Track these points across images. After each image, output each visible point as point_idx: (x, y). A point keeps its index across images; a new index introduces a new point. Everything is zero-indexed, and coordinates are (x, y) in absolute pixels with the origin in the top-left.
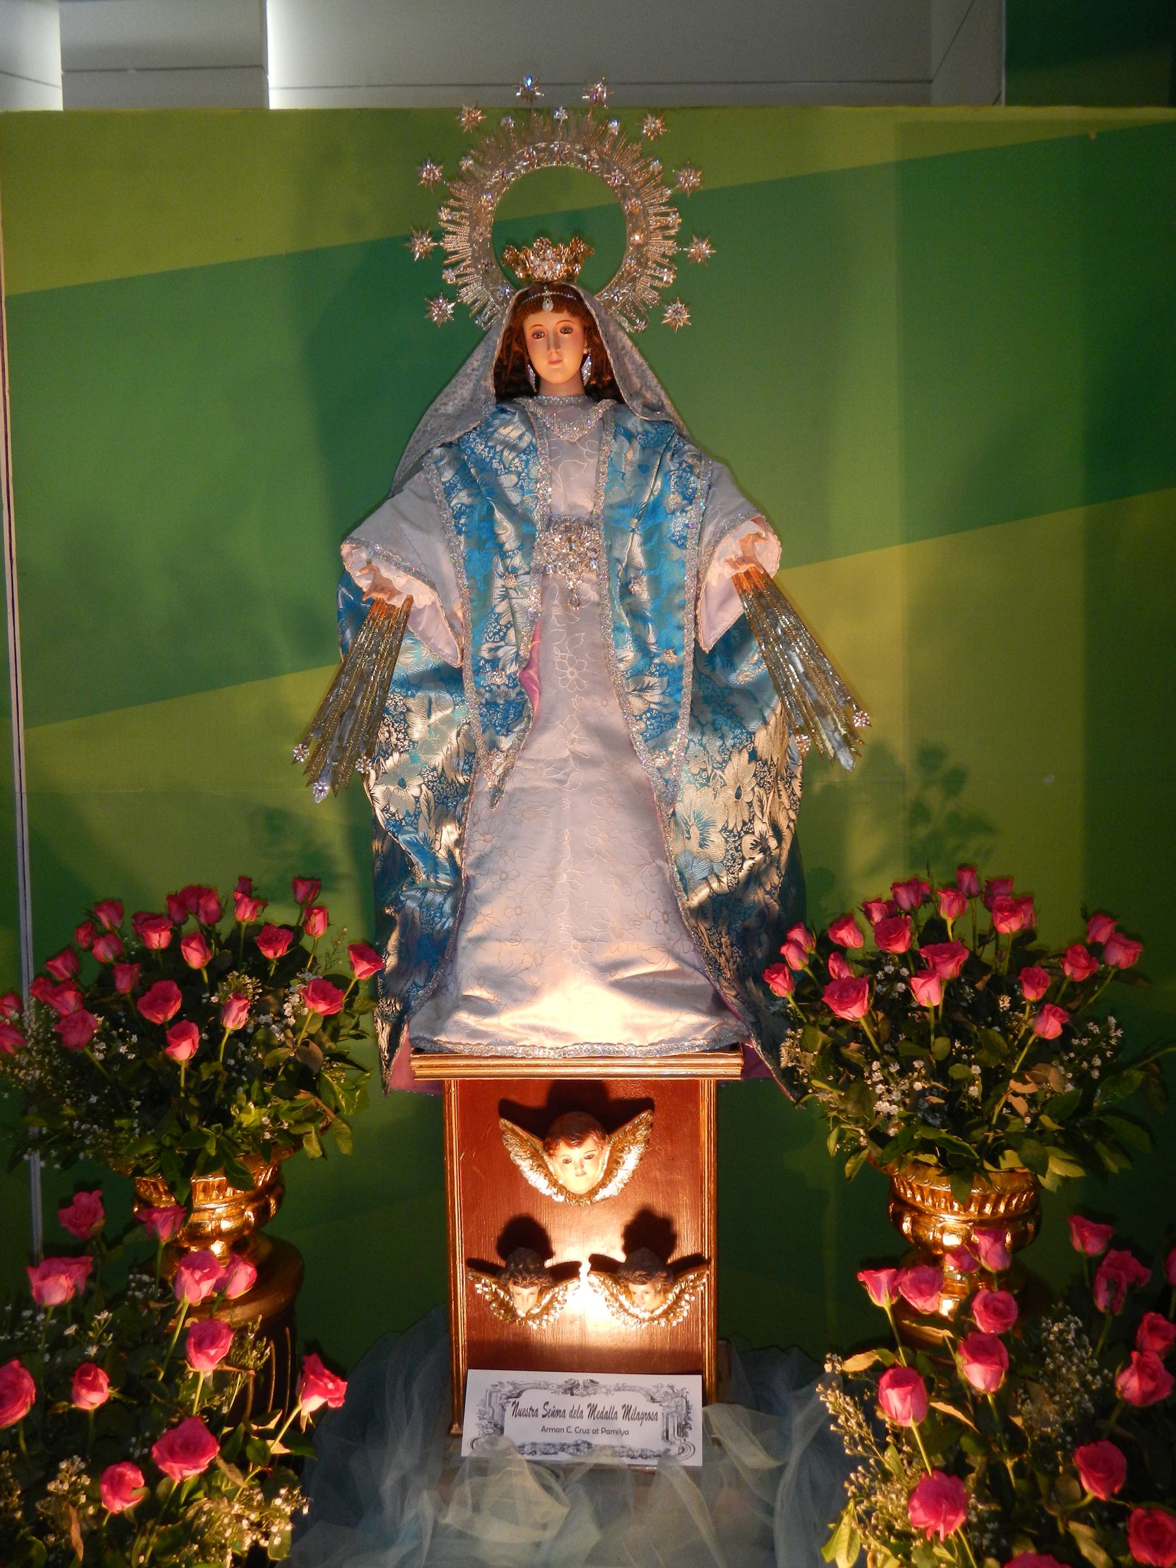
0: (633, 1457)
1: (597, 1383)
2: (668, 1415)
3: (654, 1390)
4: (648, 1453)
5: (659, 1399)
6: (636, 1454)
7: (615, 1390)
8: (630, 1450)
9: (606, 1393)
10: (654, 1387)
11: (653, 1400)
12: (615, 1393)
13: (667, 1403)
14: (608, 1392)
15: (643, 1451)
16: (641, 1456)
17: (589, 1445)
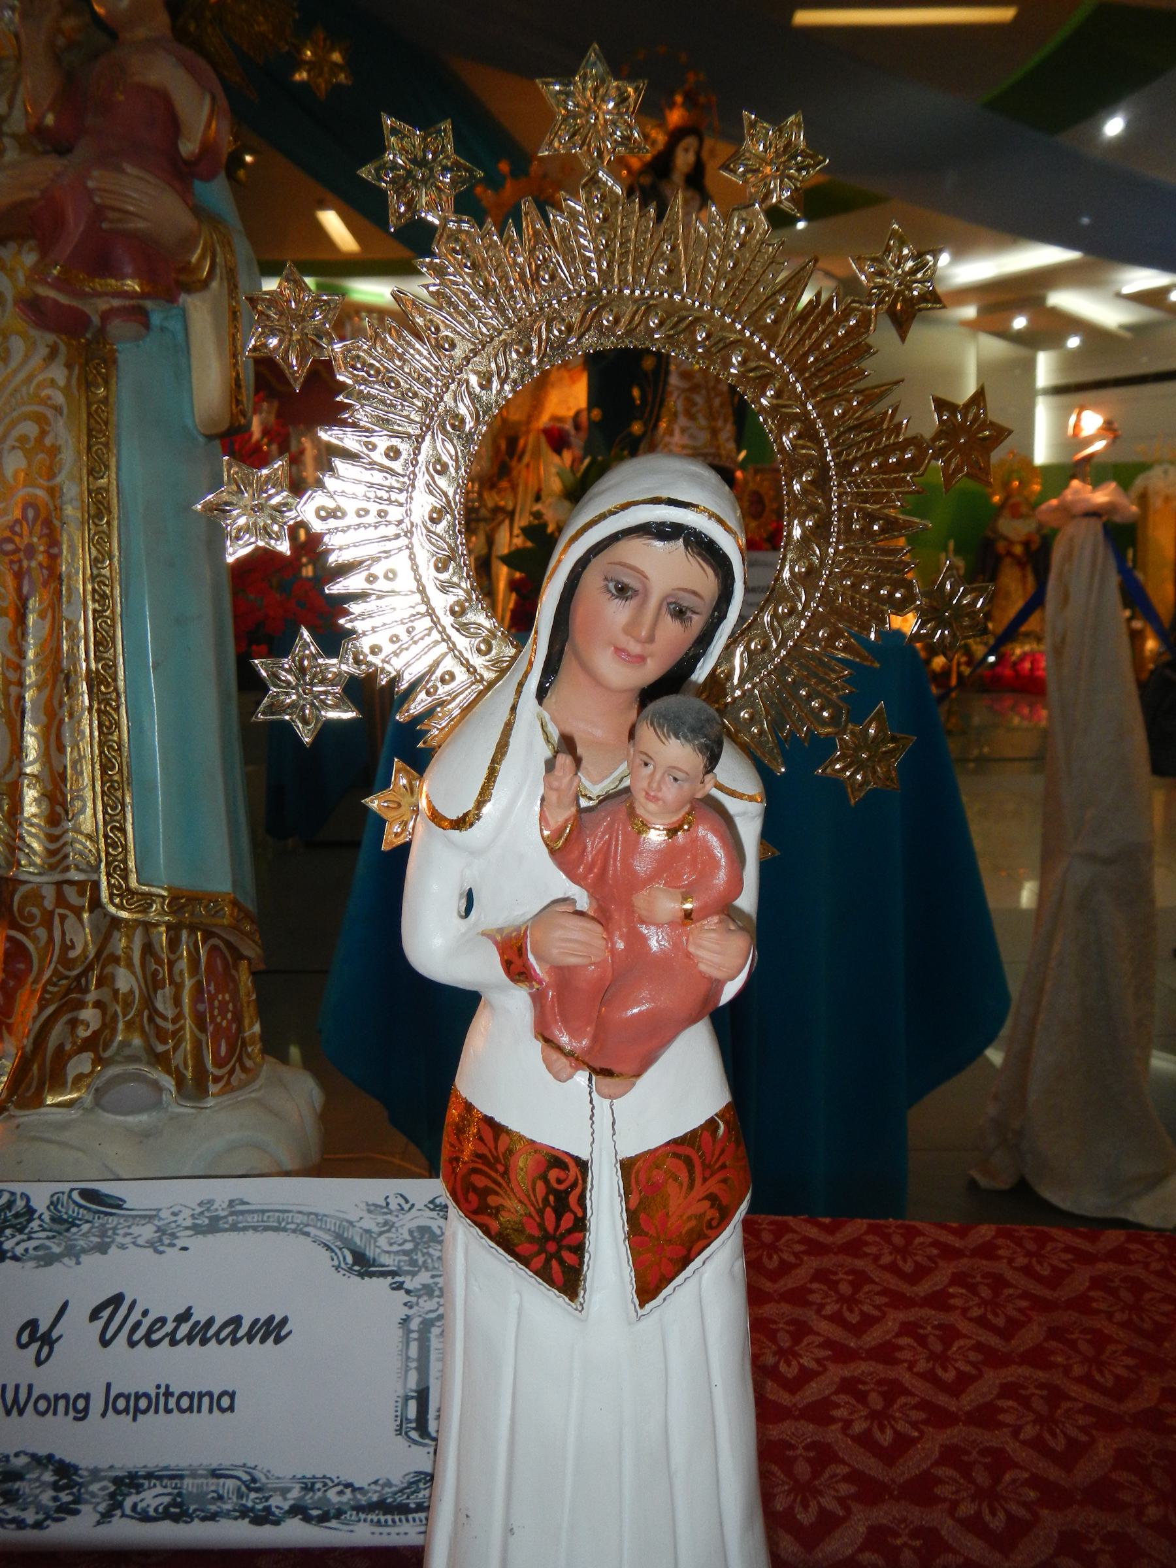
0: (263, 1518)
1: (117, 1204)
2: (427, 1325)
3: (369, 1223)
4: (332, 1495)
5: (389, 1261)
6: (277, 1503)
7: (197, 1230)
8: (252, 1484)
9: (154, 1246)
10: (372, 1208)
11: (363, 1265)
12: (197, 1243)
13: (424, 1278)
14: (163, 1239)
15: (308, 1487)
16: (298, 1510)
17: (65, 1471)
